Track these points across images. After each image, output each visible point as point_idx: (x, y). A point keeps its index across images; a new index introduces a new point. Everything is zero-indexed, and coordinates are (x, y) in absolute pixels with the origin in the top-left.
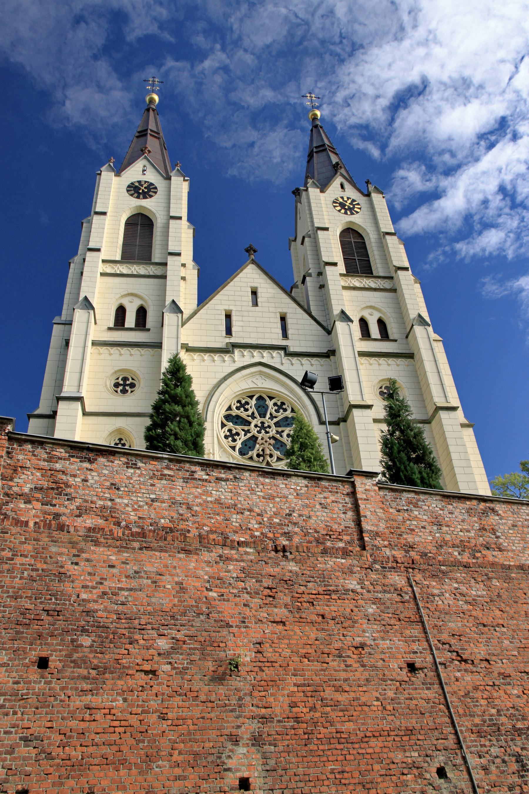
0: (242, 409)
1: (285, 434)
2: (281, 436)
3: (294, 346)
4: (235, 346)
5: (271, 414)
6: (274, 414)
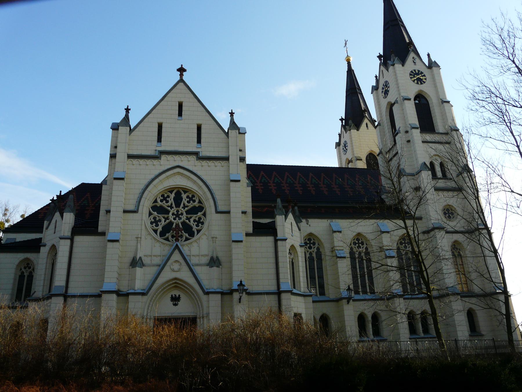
0: (164, 202)
1: (192, 220)
2: (190, 221)
3: (205, 150)
4: (162, 153)
5: (184, 204)
6: (186, 204)
